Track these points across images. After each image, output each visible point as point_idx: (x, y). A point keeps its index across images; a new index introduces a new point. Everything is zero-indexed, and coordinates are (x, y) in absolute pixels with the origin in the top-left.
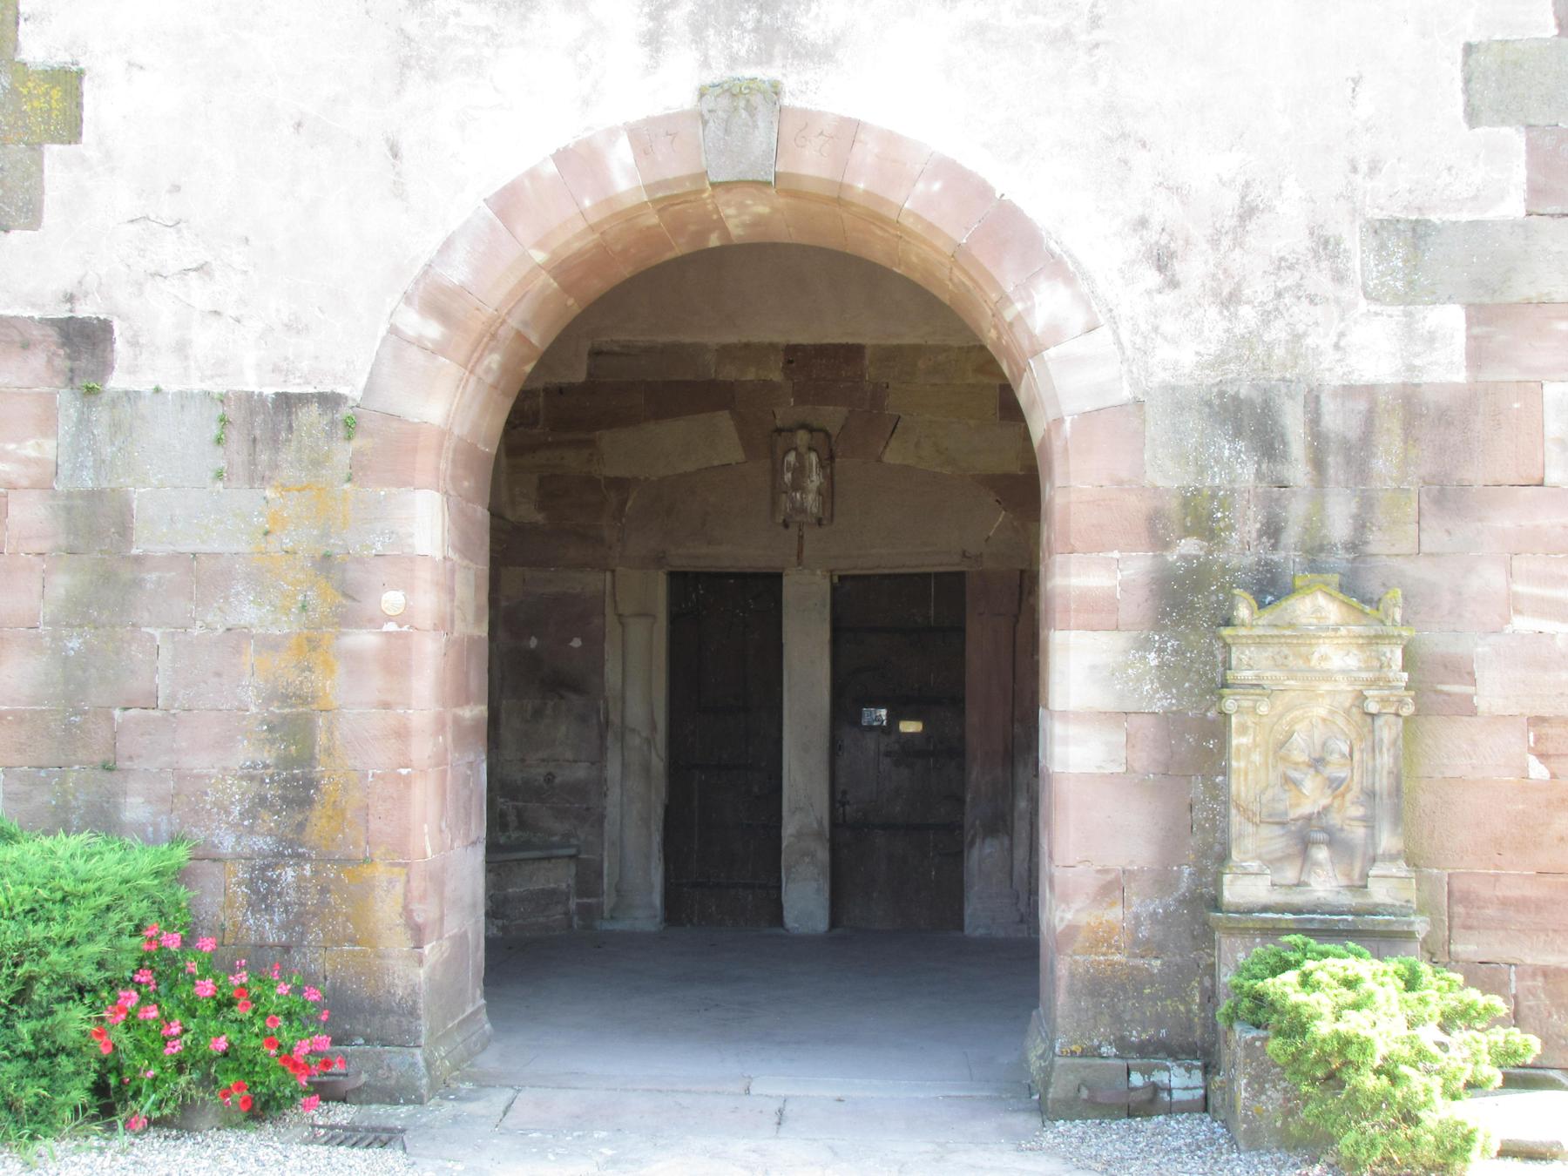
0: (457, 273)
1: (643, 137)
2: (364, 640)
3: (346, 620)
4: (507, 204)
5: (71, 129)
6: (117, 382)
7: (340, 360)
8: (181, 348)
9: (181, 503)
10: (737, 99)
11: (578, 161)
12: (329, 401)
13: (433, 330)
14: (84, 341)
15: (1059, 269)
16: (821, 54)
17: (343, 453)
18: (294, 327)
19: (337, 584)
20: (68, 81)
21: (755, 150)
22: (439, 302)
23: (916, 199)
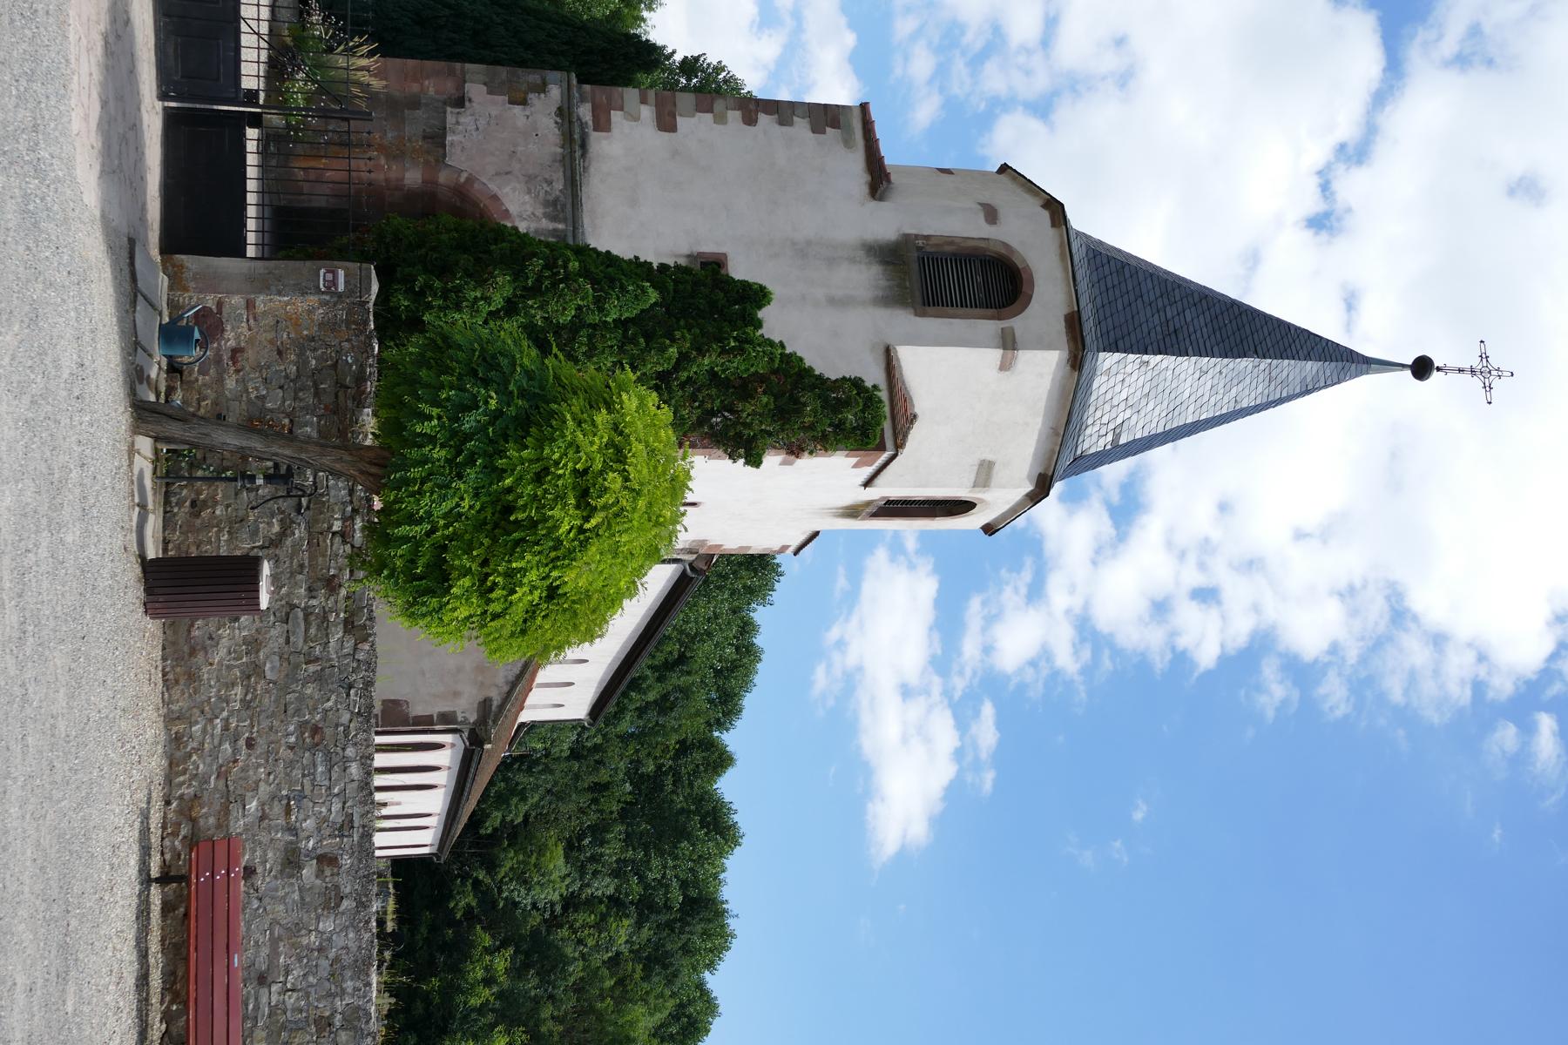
0: (476, 186)
2: (383, 161)
3: (387, 157)
4: (495, 198)
5: (510, 102)
6: (449, 109)
7: (455, 158)
8: (458, 123)
12: (445, 156)
13: (462, 180)
14: (460, 102)
17: (431, 159)
18: (463, 149)
19: (397, 153)
20: (524, 102)
22: (471, 180)
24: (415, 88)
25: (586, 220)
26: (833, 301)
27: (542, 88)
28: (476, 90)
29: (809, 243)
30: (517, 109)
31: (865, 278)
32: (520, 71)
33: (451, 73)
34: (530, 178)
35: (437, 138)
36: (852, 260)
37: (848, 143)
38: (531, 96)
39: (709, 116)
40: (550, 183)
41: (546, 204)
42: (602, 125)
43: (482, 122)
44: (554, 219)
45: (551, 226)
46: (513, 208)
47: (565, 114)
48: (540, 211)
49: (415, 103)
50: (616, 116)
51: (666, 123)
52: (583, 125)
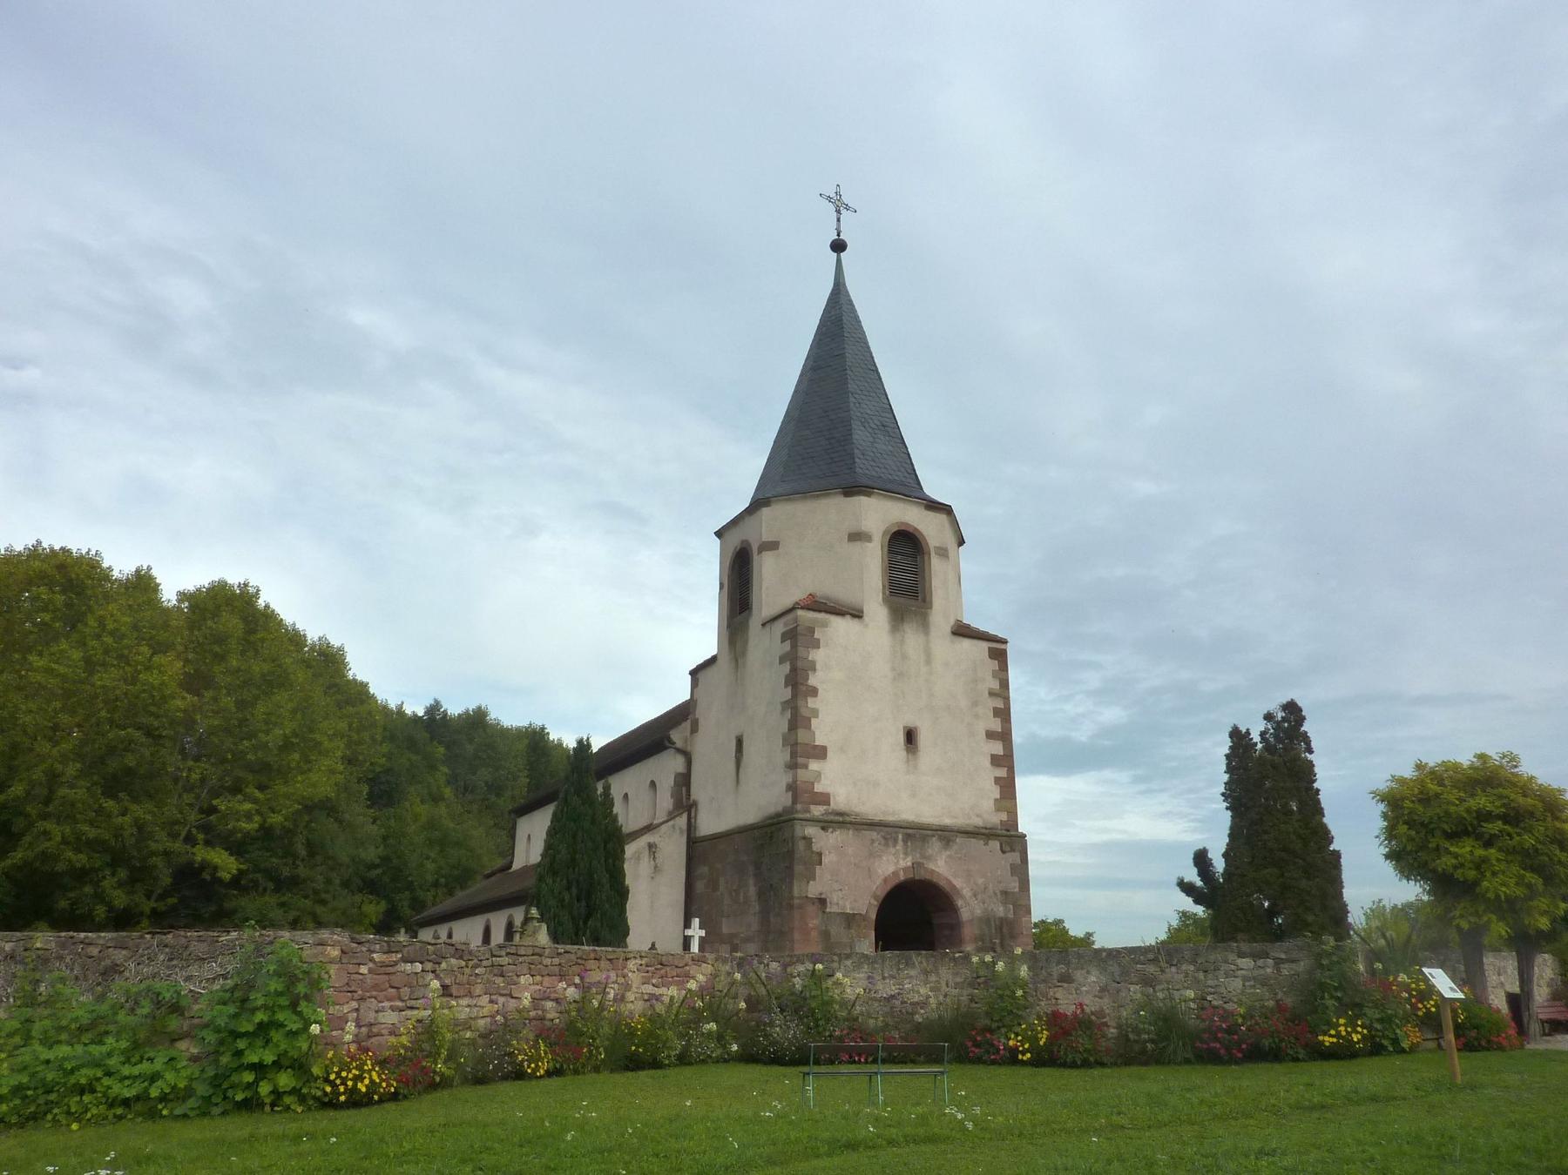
1: (905, 869)
4: (885, 880)
9: (837, 930)
10: (916, 866)
11: (895, 873)
14: (822, 902)
15: (962, 897)
16: (929, 858)
20: (820, 854)
21: (921, 875)
22: (875, 897)
23: (942, 883)
24: (814, 934)
25: (890, 818)
26: (928, 661)
27: (808, 840)
28: (813, 889)
29: (893, 669)
30: (825, 860)
31: (912, 639)
32: (797, 856)
33: (800, 907)
34: (871, 855)
35: (850, 919)
36: (902, 642)
37: (825, 625)
38: (815, 848)
39: (813, 721)
40: (873, 841)
41: (887, 845)
42: (824, 799)
43: (836, 886)
44: (896, 841)
45: (900, 842)
46: (891, 869)
47: (825, 825)
48: (892, 850)
49: (826, 935)
50: (818, 788)
51: (821, 753)
52: (827, 813)
